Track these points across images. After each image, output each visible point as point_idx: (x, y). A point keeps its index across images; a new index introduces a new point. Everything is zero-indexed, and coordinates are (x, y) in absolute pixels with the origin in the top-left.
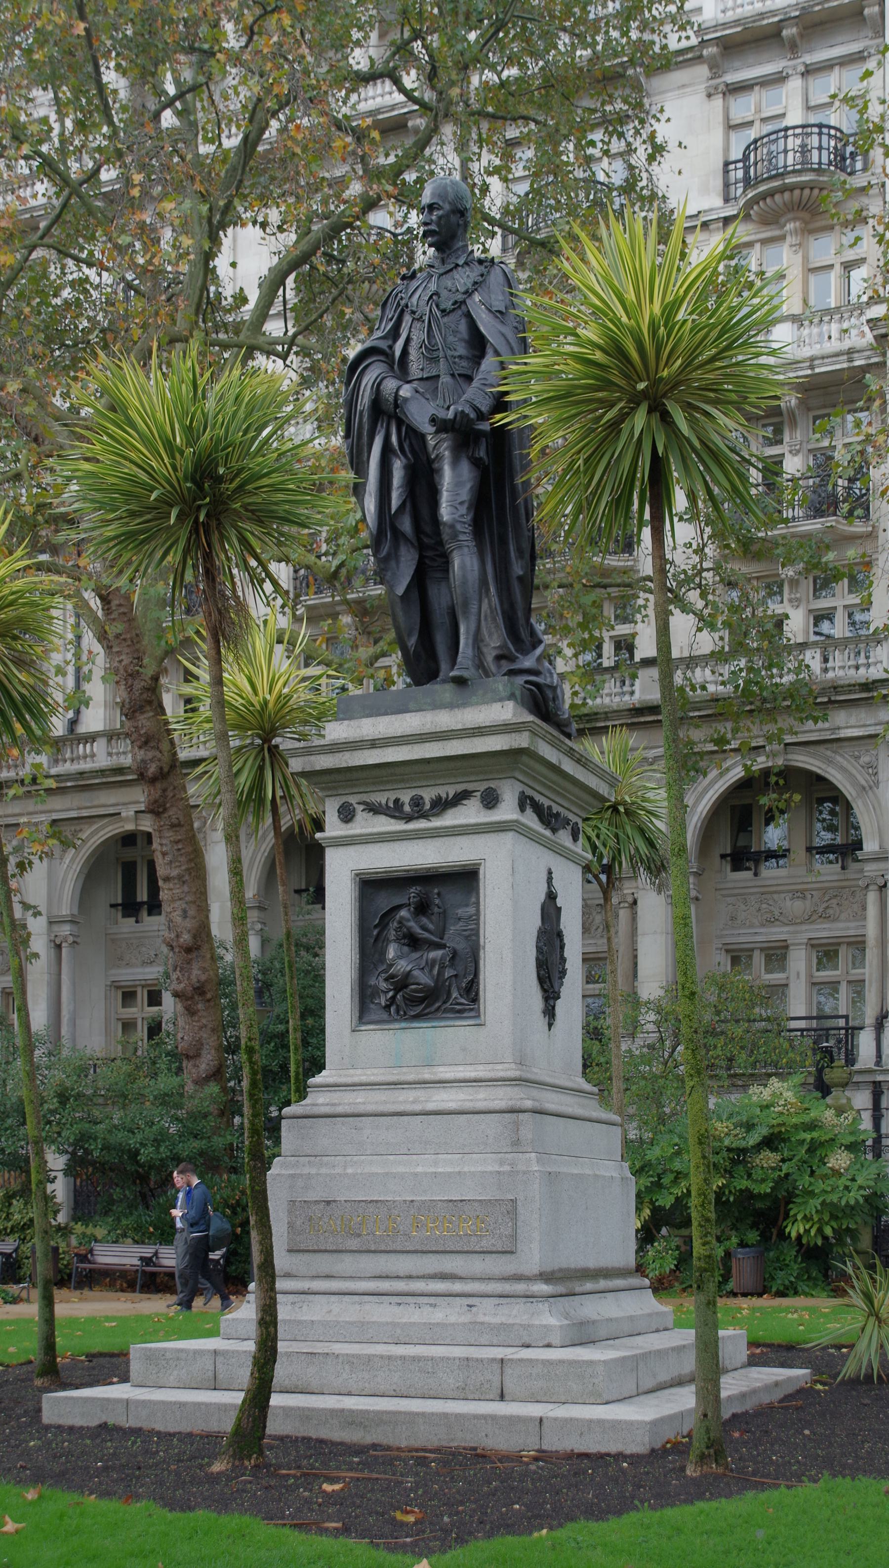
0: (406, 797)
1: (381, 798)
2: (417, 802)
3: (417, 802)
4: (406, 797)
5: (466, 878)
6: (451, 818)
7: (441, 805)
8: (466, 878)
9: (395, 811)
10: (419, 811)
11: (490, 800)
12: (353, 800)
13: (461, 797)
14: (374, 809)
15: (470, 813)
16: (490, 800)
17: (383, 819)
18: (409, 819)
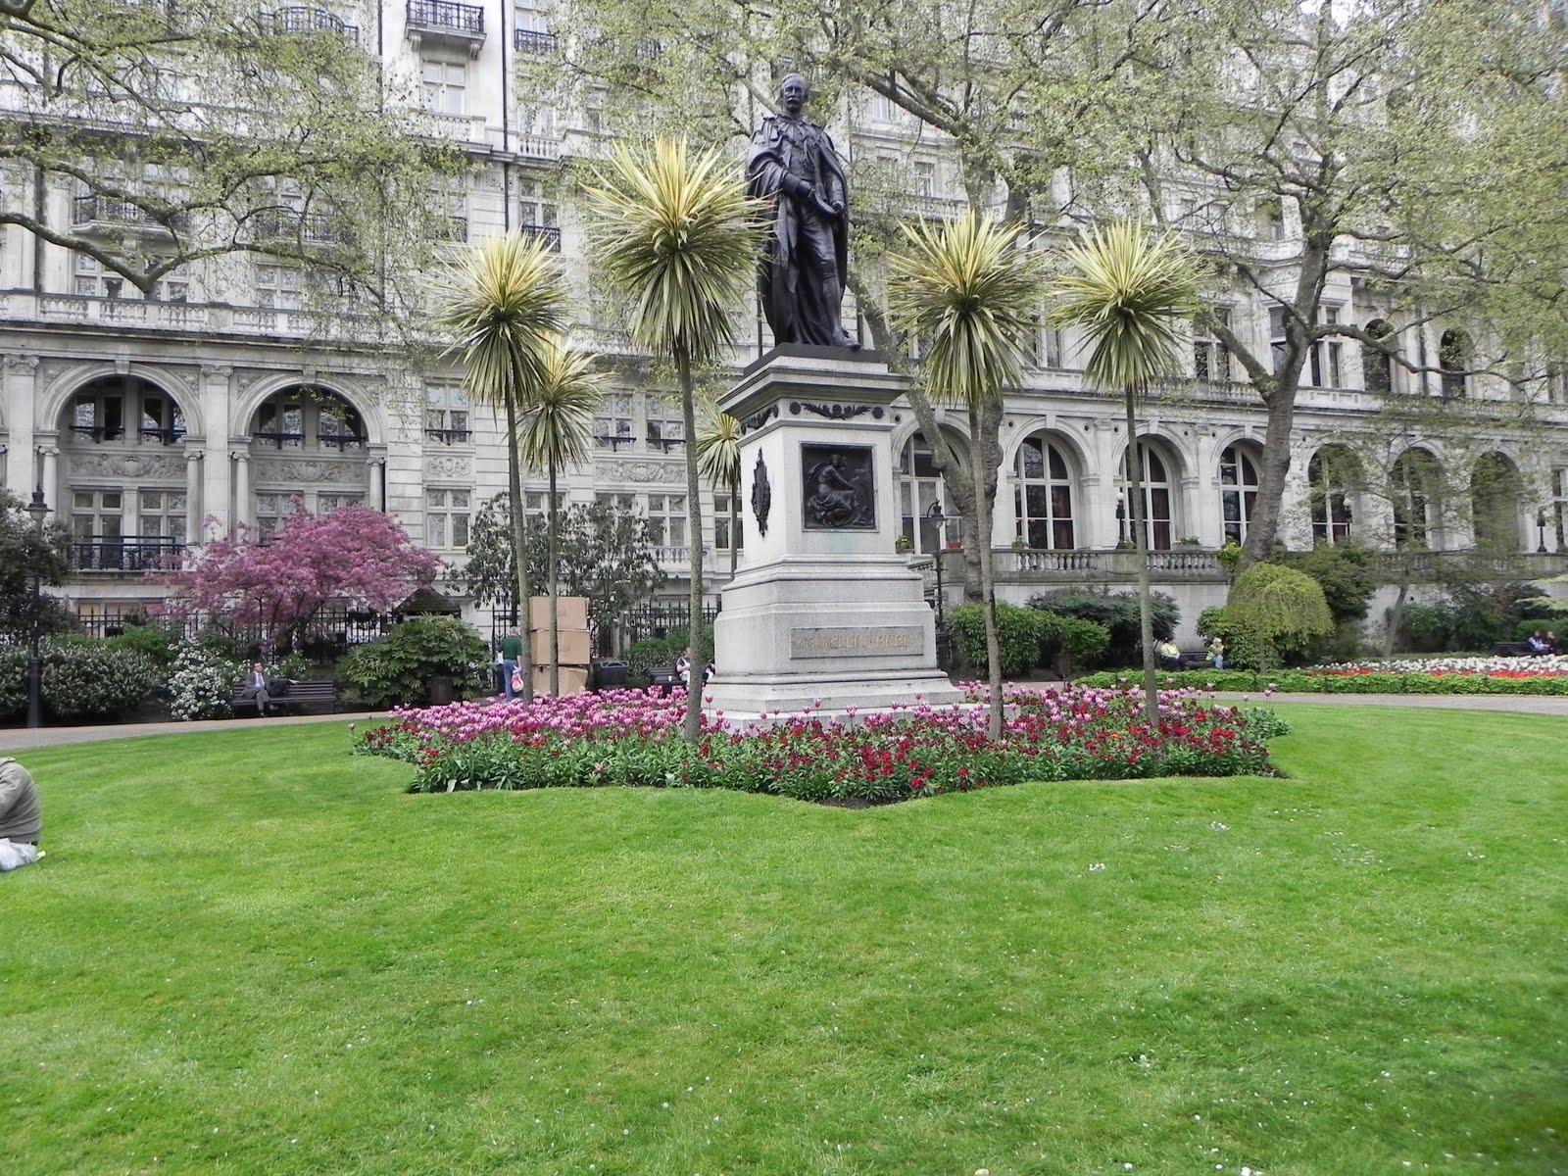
0: (830, 406)
1: (817, 404)
2: (837, 408)
3: (837, 408)
4: (830, 406)
5: (864, 454)
6: (856, 420)
7: (850, 413)
8: (864, 454)
9: (824, 412)
10: (836, 413)
11: (878, 414)
12: (799, 402)
13: (861, 411)
14: (813, 409)
15: (867, 419)
16: (878, 414)
17: (817, 415)
18: (833, 417)
